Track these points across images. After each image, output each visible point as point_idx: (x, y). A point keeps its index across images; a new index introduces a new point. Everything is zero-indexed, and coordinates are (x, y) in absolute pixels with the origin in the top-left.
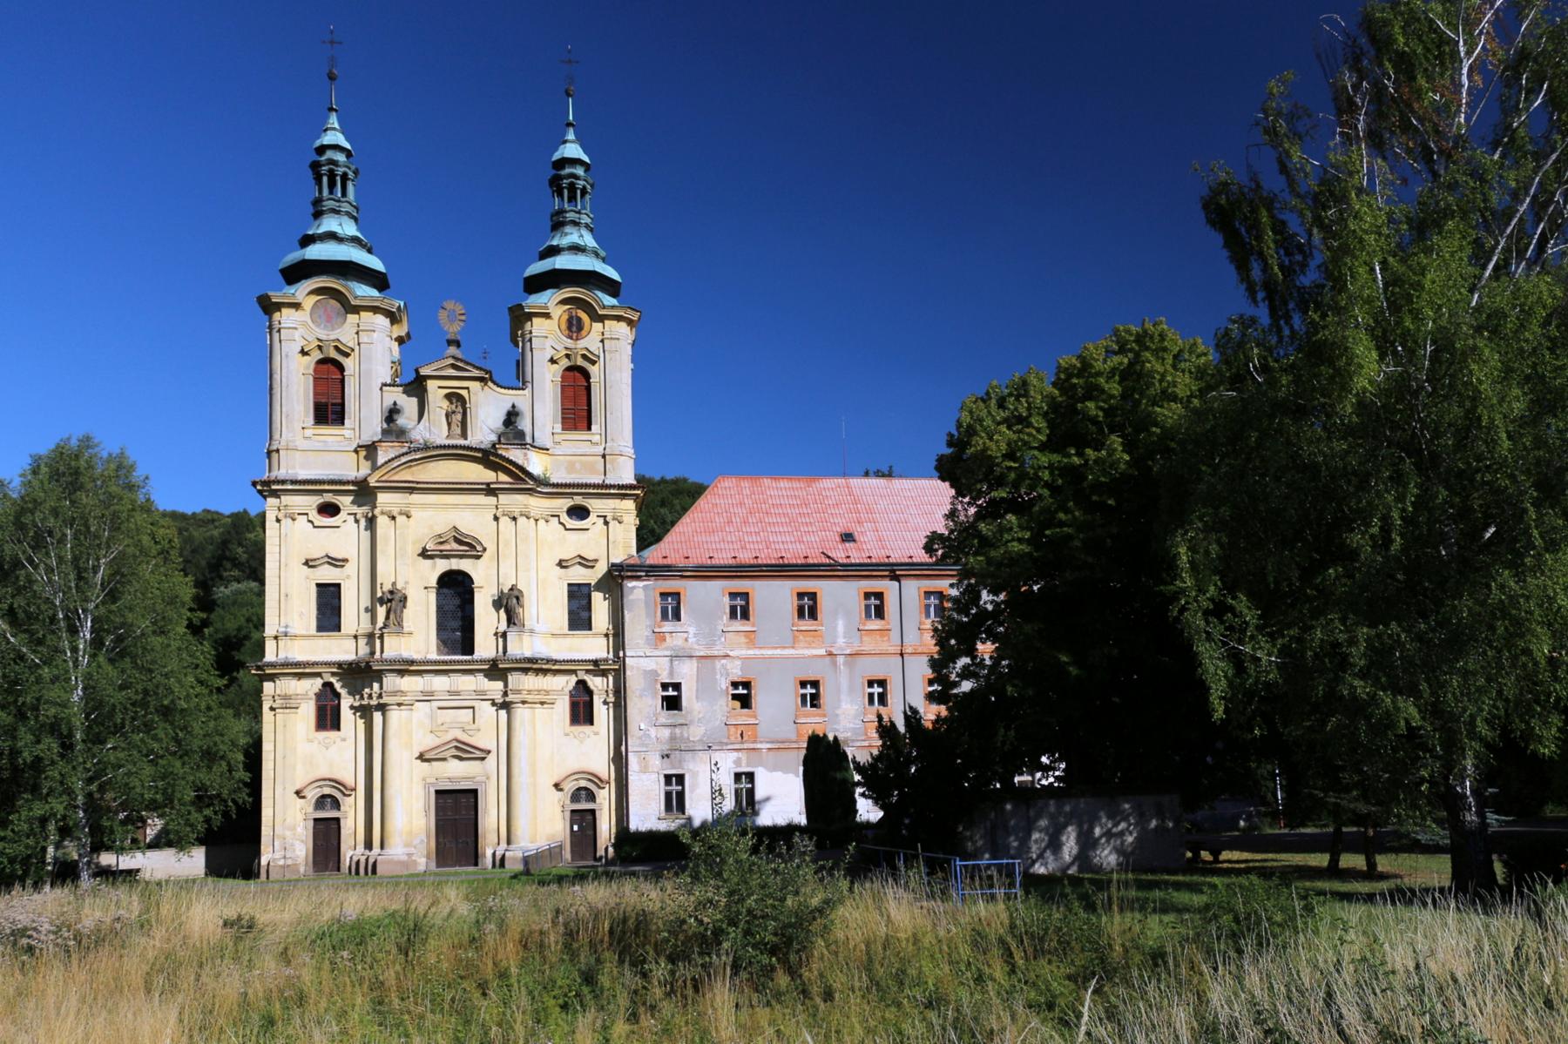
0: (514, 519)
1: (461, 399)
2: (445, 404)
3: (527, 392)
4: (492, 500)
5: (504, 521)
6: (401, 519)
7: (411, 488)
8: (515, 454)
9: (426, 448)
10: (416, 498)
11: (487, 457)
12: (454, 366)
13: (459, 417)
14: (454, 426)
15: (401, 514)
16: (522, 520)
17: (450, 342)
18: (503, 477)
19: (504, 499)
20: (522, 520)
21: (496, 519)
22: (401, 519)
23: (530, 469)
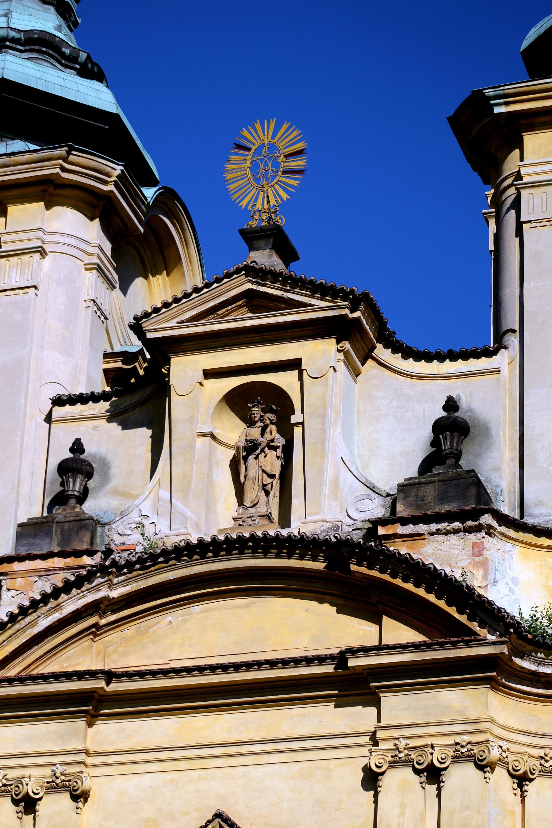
0: (433, 775)
1: (279, 405)
2: (234, 431)
3: (502, 360)
4: (361, 717)
5: (401, 783)
6: (53, 806)
7: (92, 702)
8: (445, 552)
9: (151, 559)
10: (110, 733)
11: (348, 572)
12: (254, 301)
13: (272, 462)
14: (252, 493)
15: (53, 787)
16: (461, 778)
17: (252, 238)
18: (397, 632)
19: (398, 706)
20: (461, 778)
21: (371, 780)
22: (53, 806)
23: (499, 596)
